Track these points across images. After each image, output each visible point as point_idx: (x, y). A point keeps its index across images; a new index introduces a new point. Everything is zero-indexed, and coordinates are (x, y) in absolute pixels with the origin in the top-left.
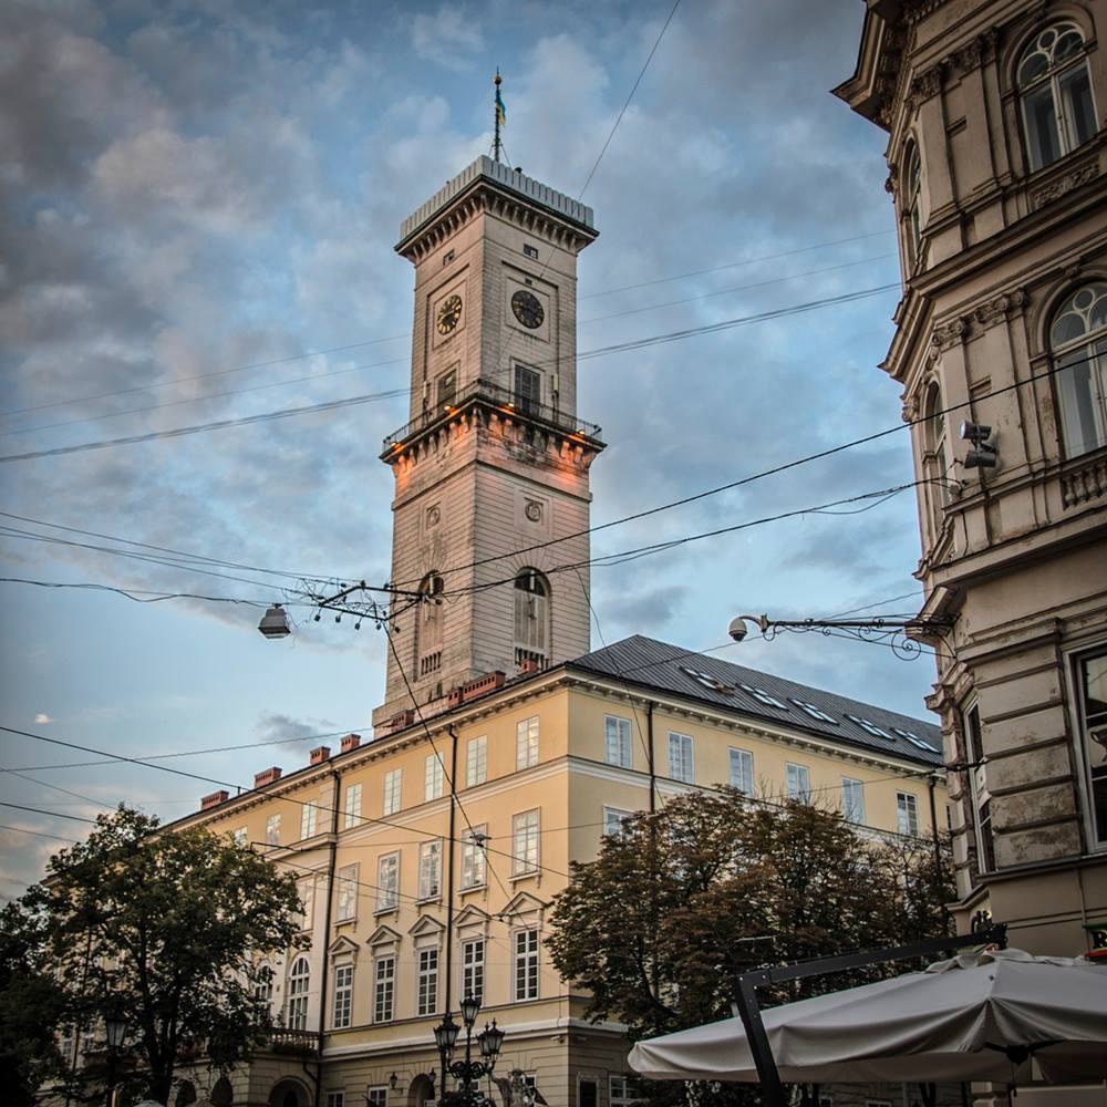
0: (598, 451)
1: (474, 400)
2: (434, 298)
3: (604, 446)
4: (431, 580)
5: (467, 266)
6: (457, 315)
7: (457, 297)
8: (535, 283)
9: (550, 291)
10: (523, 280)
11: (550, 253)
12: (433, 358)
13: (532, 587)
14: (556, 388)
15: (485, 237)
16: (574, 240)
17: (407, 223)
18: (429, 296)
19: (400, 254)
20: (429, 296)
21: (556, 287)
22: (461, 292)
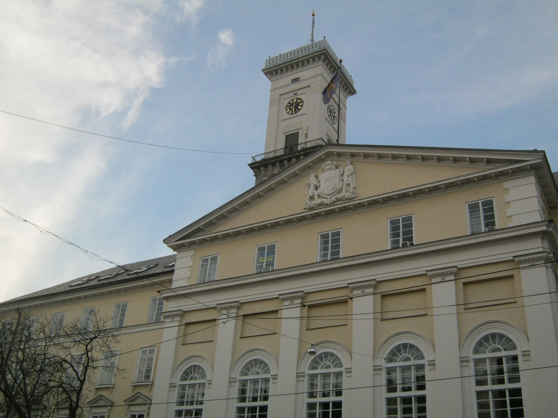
5: (310, 86)
6: (300, 107)
7: (300, 99)
16: (348, 91)
17: (269, 61)
19: (264, 73)
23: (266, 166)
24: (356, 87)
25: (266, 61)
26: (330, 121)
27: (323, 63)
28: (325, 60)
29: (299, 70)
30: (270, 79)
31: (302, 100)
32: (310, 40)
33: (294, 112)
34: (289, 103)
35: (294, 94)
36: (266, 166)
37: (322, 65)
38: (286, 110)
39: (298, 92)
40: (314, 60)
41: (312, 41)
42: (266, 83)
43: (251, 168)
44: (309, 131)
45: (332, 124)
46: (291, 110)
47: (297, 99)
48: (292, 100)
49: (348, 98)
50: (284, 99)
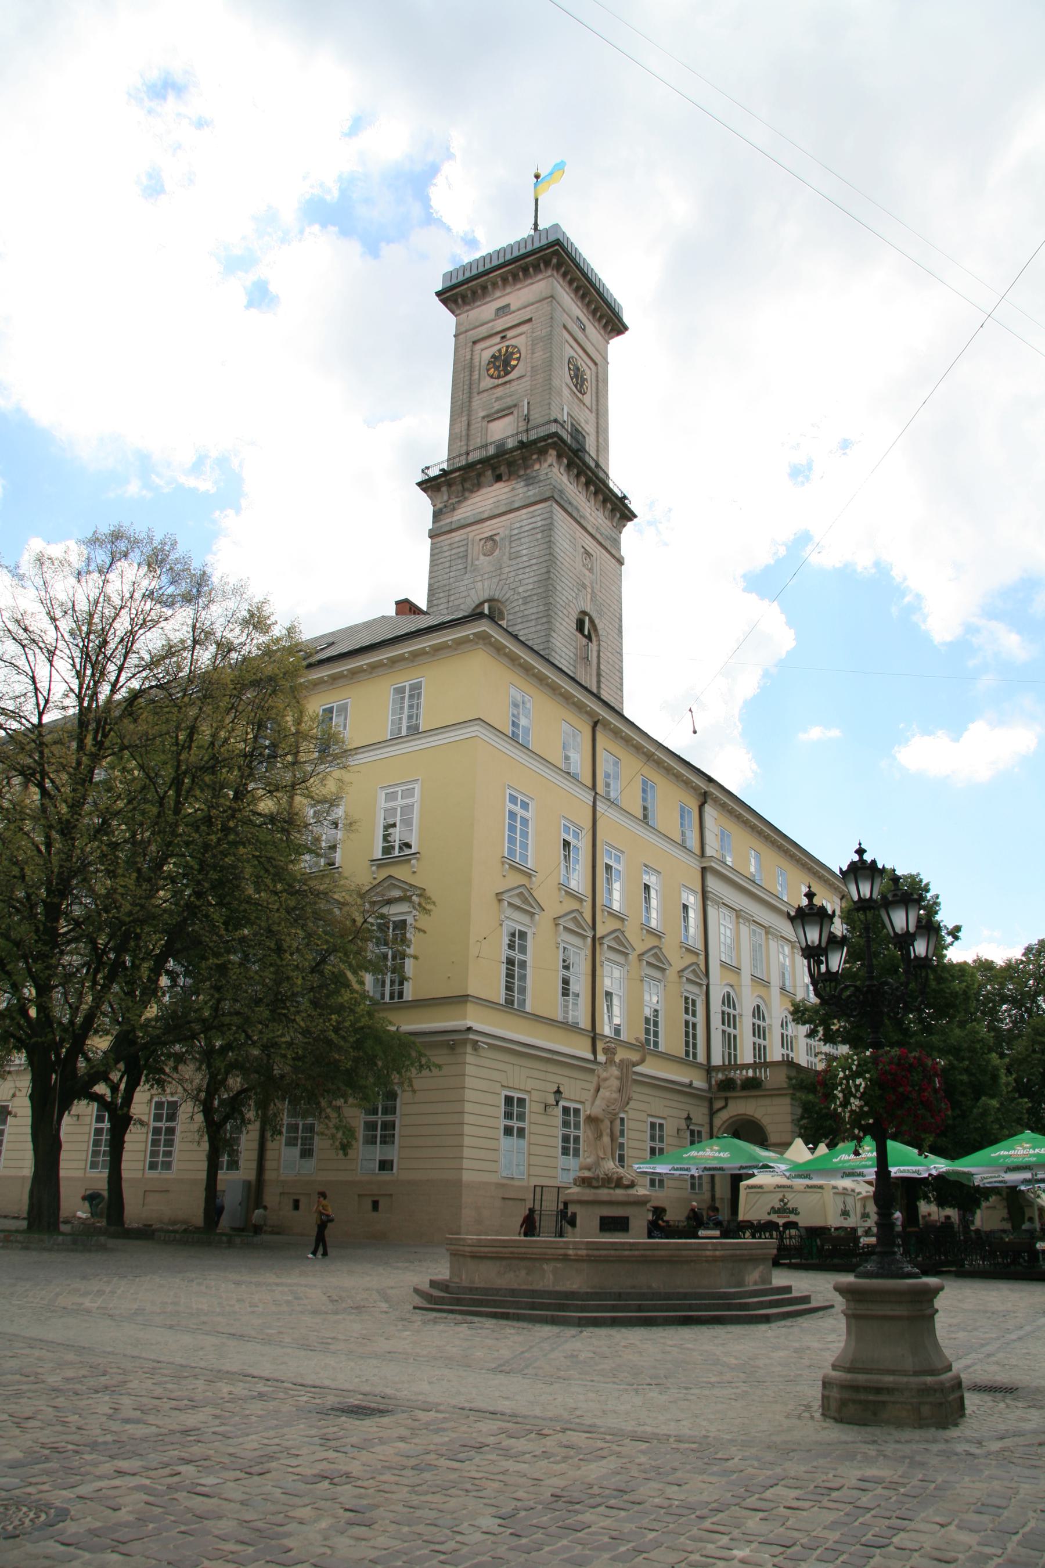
0: (630, 520)
1: (556, 439)
3: (635, 516)
4: (486, 605)
5: (530, 320)
6: (514, 363)
11: (593, 331)
13: (586, 633)
17: (449, 275)
18: (474, 343)
20: (474, 343)
23: (450, 484)
24: (626, 319)
26: (574, 388)
28: (558, 267)
29: (508, 290)
30: (453, 312)
33: (502, 373)
34: (493, 356)
35: (503, 337)
37: (552, 276)
38: (488, 370)
39: (510, 334)
40: (537, 269)
41: (536, 228)
42: (446, 320)
43: (423, 489)
44: (532, 408)
46: (497, 368)
47: (508, 347)
48: (500, 351)
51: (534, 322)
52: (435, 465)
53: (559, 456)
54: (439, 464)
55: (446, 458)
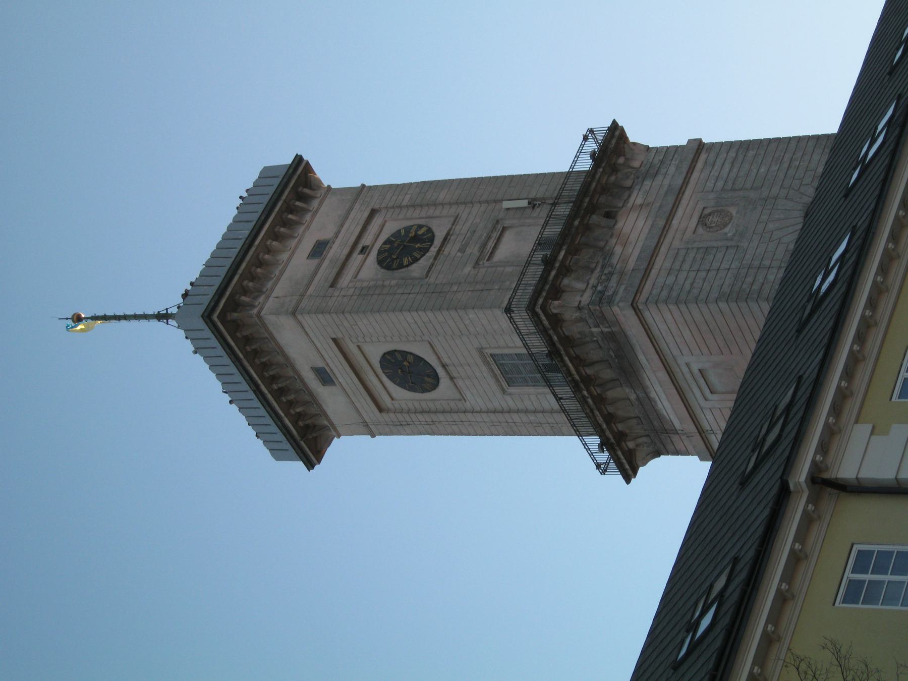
2: (386, 400)
3: (615, 124)
6: (410, 358)
8: (367, 240)
9: (377, 221)
10: (361, 257)
12: (473, 400)
14: (524, 203)
15: (293, 313)
16: (306, 191)
17: (278, 454)
18: (381, 410)
19: (319, 462)
21: (373, 212)
22: (376, 352)
23: (621, 437)
25: (278, 458)
27: (255, 311)
31: (388, 357)
32: (167, 323)
36: (621, 437)
45: (437, 242)
49: (326, 184)
50: (392, 399)
51: (340, 335)
52: (594, 459)
53: (557, 292)
54: (591, 454)
55: (575, 439)
